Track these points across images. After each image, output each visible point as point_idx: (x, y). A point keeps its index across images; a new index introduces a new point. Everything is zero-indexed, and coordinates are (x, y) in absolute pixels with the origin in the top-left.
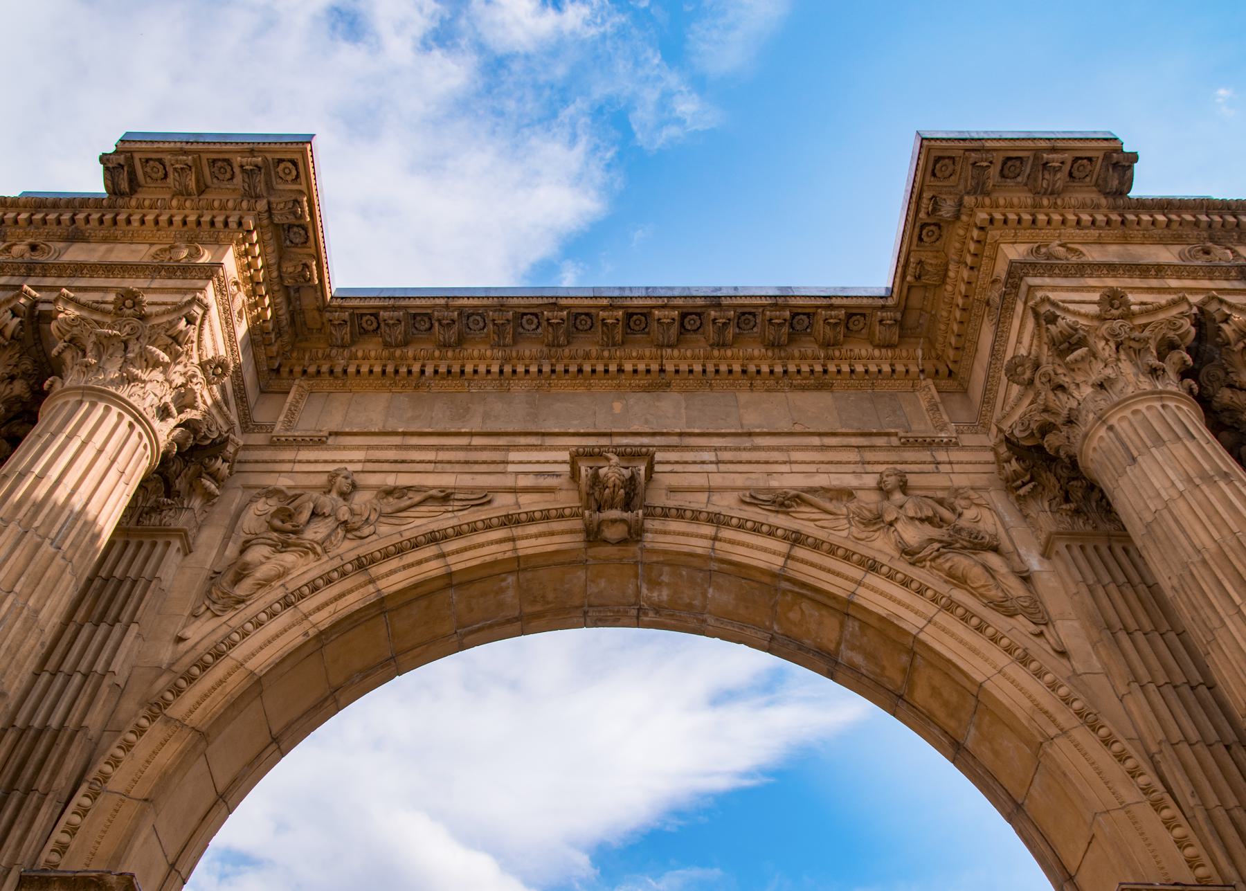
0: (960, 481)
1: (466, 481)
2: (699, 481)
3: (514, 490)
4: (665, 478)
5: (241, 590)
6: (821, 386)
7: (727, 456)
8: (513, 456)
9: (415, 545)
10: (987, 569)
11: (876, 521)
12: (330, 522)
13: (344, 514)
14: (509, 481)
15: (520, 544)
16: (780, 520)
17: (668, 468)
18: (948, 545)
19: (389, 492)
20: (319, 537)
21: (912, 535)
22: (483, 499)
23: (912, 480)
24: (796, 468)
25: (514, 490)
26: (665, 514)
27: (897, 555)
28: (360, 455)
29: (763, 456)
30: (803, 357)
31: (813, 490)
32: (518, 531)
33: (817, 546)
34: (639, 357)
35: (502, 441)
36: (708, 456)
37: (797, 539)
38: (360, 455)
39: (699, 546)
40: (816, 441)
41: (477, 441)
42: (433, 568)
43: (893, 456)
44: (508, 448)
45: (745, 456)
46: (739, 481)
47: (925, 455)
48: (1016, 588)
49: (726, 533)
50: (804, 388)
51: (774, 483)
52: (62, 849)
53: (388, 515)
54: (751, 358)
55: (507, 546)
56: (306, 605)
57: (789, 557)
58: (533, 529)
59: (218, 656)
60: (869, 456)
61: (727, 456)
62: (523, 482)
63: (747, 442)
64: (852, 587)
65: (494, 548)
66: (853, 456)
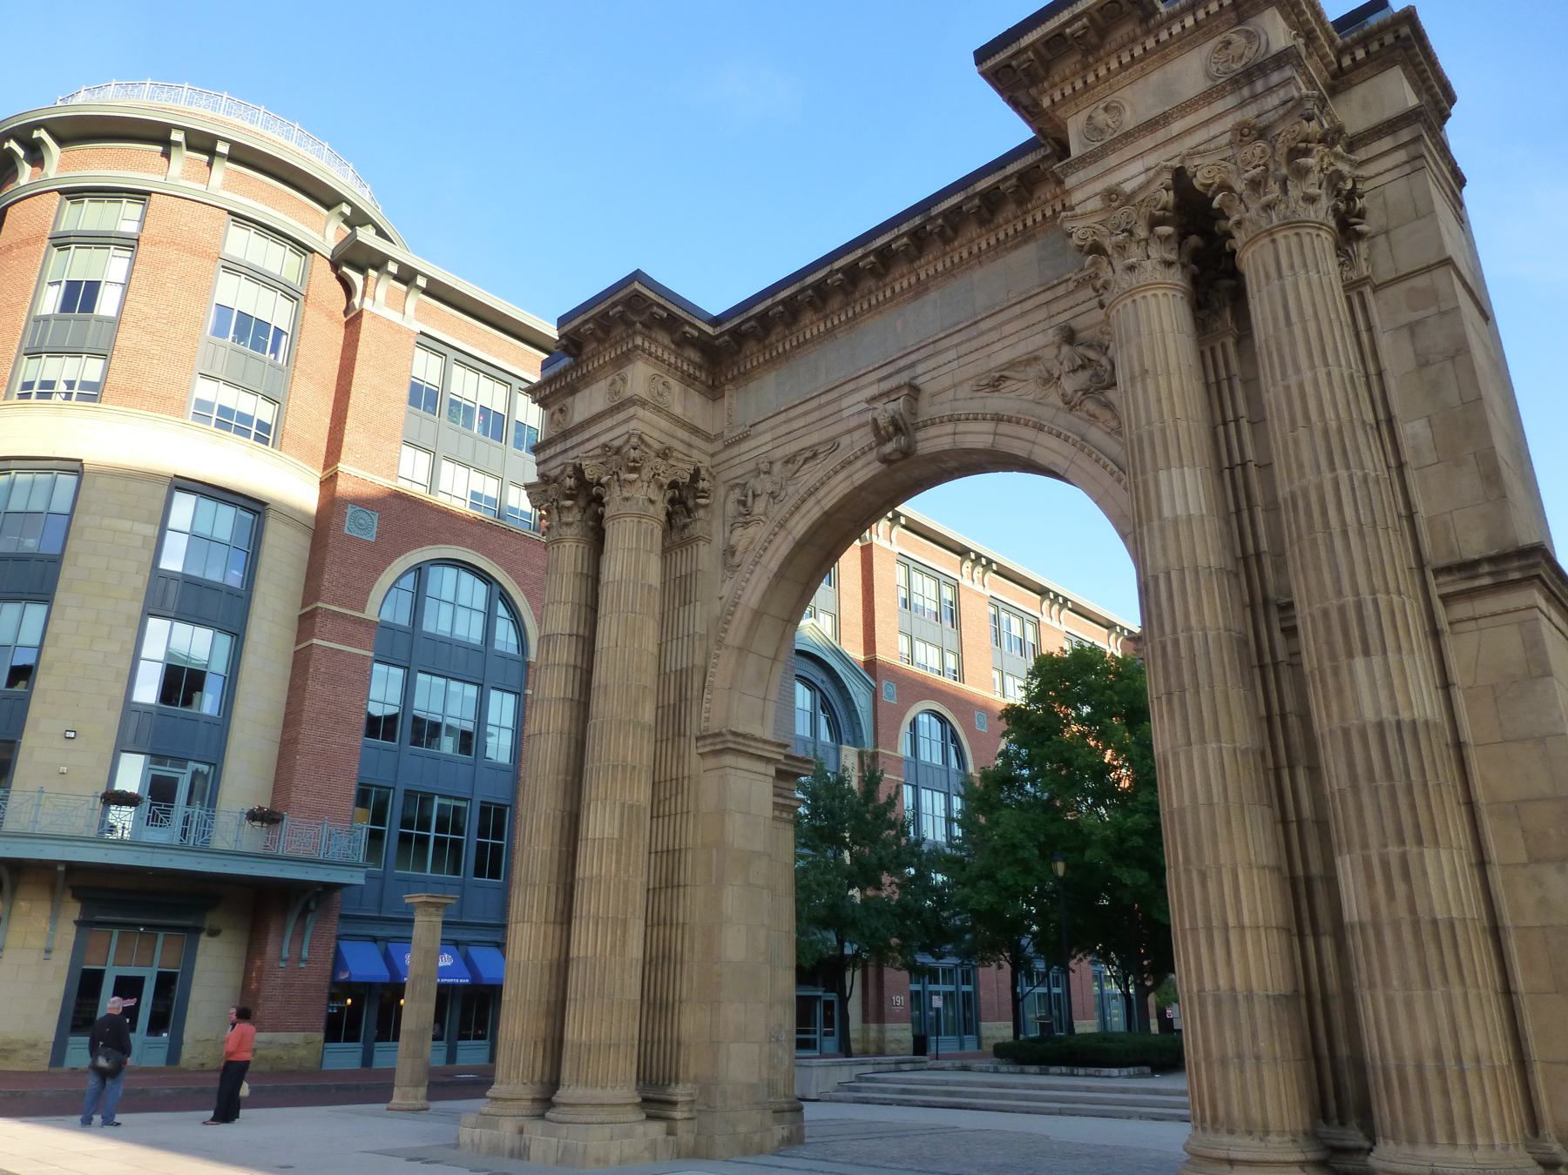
3: (849, 432)
5: (737, 559)
6: (1026, 241)
7: (963, 349)
8: (846, 402)
11: (1049, 380)
12: (764, 497)
13: (769, 488)
15: (855, 477)
17: (928, 377)
19: (789, 460)
20: (761, 510)
22: (833, 445)
23: (1078, 324)
25: (849, 432)
27: (1061, 404)
28: (768, 437)
30: (1007, 222)
31: (1012, 365)
32: (852, 468)
34: (901, 279)
35: (835, 394)
36: (952, 354)
37: (998, 418)
39: (945, 443)
40: (1017, 310)
42: (816, 513)
43: (1070, 301)
44: (840, 398)
45: (975, 344)
46: (971, 370)
49: (961, 427)
50: (1016, 247)
51: (992, 364)
52: (707, 719)
53: (790, 479)
54: (972, 241)
55: (848, 483)
56: (764, 560)
57: (995, 434)
58: (859, 464)
59: (736, 605)
60: (1055, 308)
61: (963, 349)
63: (973, 331)
64: (1028, 446)
65: (843, 485)
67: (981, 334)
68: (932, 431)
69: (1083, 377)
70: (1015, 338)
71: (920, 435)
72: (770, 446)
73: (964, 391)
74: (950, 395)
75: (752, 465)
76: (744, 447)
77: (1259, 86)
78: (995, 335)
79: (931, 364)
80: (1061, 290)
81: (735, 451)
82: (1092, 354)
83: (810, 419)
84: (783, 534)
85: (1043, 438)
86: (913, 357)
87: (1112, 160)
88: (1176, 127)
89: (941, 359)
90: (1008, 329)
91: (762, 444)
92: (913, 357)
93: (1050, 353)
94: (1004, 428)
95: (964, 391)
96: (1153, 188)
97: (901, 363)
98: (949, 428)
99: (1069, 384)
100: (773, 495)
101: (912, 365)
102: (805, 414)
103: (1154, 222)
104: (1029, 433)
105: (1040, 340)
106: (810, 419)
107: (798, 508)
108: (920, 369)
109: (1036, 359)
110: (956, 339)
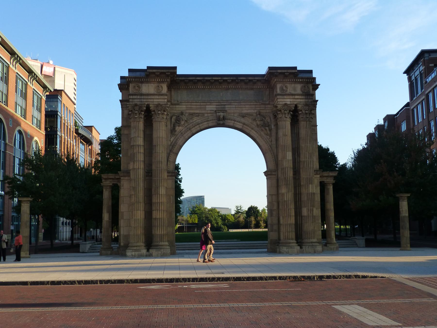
0: (268, 111)
1: (201, 112)
2: (232, 111)
3: (207, 113)
4: (229, 111)
7: (237, 106)
8: (207, 107)
9: (196, 125)
10: (266, 130)
11: (255, 120)
14: (206, 112)
16: (243, 120)
18: (262, 125)
21: (259, 123)
23: (262, 111)
24: (246, 109)
25: (207, 113)
26: (228, 119)
29: (242, 106)
32: (209, 122)
33: (246, 125)
36: (234, 106)
37: (244, 124)
38: (185, 107)
40: (249, 103)
41: (202, 104)
44: (206, 105)
45: (239, 106)
47: (264, 106)
48: (269, 132)
49: (235, 123)
61: (237, 106)
62: (209, 112)
66: (254, 106)
67: (241, 105)
68: (229, 121)
69: (262, 122)
70: (248, 109)
71: (226, 121)
72: (185, 109)
73: (236, 115)
74: (233, 114)
75: (180, 112)
76: (177, 106)
77: (309, 97)
78: (244, 106)
79: (229, 106)
80: (258, 103)
81: (174, 106)
82: (264, 119)
83: (198, 107)
84: (189, 131)
85: (252, 131)
86: (225, 103)
87: (285, 97)
88: (296, 97)
89: (232, 106)
90: (247, 106)
91: (183, 107)
92: (225, 103)
93: (255, 115)
94: (244, 126)
95: (236, 115)
96: (291, 106)
97: (223, 104)
98: (233, 122)
99: (259, 123)
100: (186, 121)
101: (225, 105)
102: (196, 105)
103: (290, 111)
104: (250, 129)
105: (253, 111)
106: (198, 107)
107: (194, 126)
108: (226, 106)
109: (252, 115)
110: (236, 104)
